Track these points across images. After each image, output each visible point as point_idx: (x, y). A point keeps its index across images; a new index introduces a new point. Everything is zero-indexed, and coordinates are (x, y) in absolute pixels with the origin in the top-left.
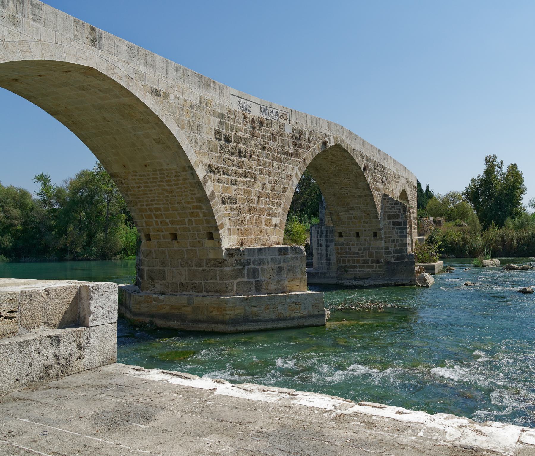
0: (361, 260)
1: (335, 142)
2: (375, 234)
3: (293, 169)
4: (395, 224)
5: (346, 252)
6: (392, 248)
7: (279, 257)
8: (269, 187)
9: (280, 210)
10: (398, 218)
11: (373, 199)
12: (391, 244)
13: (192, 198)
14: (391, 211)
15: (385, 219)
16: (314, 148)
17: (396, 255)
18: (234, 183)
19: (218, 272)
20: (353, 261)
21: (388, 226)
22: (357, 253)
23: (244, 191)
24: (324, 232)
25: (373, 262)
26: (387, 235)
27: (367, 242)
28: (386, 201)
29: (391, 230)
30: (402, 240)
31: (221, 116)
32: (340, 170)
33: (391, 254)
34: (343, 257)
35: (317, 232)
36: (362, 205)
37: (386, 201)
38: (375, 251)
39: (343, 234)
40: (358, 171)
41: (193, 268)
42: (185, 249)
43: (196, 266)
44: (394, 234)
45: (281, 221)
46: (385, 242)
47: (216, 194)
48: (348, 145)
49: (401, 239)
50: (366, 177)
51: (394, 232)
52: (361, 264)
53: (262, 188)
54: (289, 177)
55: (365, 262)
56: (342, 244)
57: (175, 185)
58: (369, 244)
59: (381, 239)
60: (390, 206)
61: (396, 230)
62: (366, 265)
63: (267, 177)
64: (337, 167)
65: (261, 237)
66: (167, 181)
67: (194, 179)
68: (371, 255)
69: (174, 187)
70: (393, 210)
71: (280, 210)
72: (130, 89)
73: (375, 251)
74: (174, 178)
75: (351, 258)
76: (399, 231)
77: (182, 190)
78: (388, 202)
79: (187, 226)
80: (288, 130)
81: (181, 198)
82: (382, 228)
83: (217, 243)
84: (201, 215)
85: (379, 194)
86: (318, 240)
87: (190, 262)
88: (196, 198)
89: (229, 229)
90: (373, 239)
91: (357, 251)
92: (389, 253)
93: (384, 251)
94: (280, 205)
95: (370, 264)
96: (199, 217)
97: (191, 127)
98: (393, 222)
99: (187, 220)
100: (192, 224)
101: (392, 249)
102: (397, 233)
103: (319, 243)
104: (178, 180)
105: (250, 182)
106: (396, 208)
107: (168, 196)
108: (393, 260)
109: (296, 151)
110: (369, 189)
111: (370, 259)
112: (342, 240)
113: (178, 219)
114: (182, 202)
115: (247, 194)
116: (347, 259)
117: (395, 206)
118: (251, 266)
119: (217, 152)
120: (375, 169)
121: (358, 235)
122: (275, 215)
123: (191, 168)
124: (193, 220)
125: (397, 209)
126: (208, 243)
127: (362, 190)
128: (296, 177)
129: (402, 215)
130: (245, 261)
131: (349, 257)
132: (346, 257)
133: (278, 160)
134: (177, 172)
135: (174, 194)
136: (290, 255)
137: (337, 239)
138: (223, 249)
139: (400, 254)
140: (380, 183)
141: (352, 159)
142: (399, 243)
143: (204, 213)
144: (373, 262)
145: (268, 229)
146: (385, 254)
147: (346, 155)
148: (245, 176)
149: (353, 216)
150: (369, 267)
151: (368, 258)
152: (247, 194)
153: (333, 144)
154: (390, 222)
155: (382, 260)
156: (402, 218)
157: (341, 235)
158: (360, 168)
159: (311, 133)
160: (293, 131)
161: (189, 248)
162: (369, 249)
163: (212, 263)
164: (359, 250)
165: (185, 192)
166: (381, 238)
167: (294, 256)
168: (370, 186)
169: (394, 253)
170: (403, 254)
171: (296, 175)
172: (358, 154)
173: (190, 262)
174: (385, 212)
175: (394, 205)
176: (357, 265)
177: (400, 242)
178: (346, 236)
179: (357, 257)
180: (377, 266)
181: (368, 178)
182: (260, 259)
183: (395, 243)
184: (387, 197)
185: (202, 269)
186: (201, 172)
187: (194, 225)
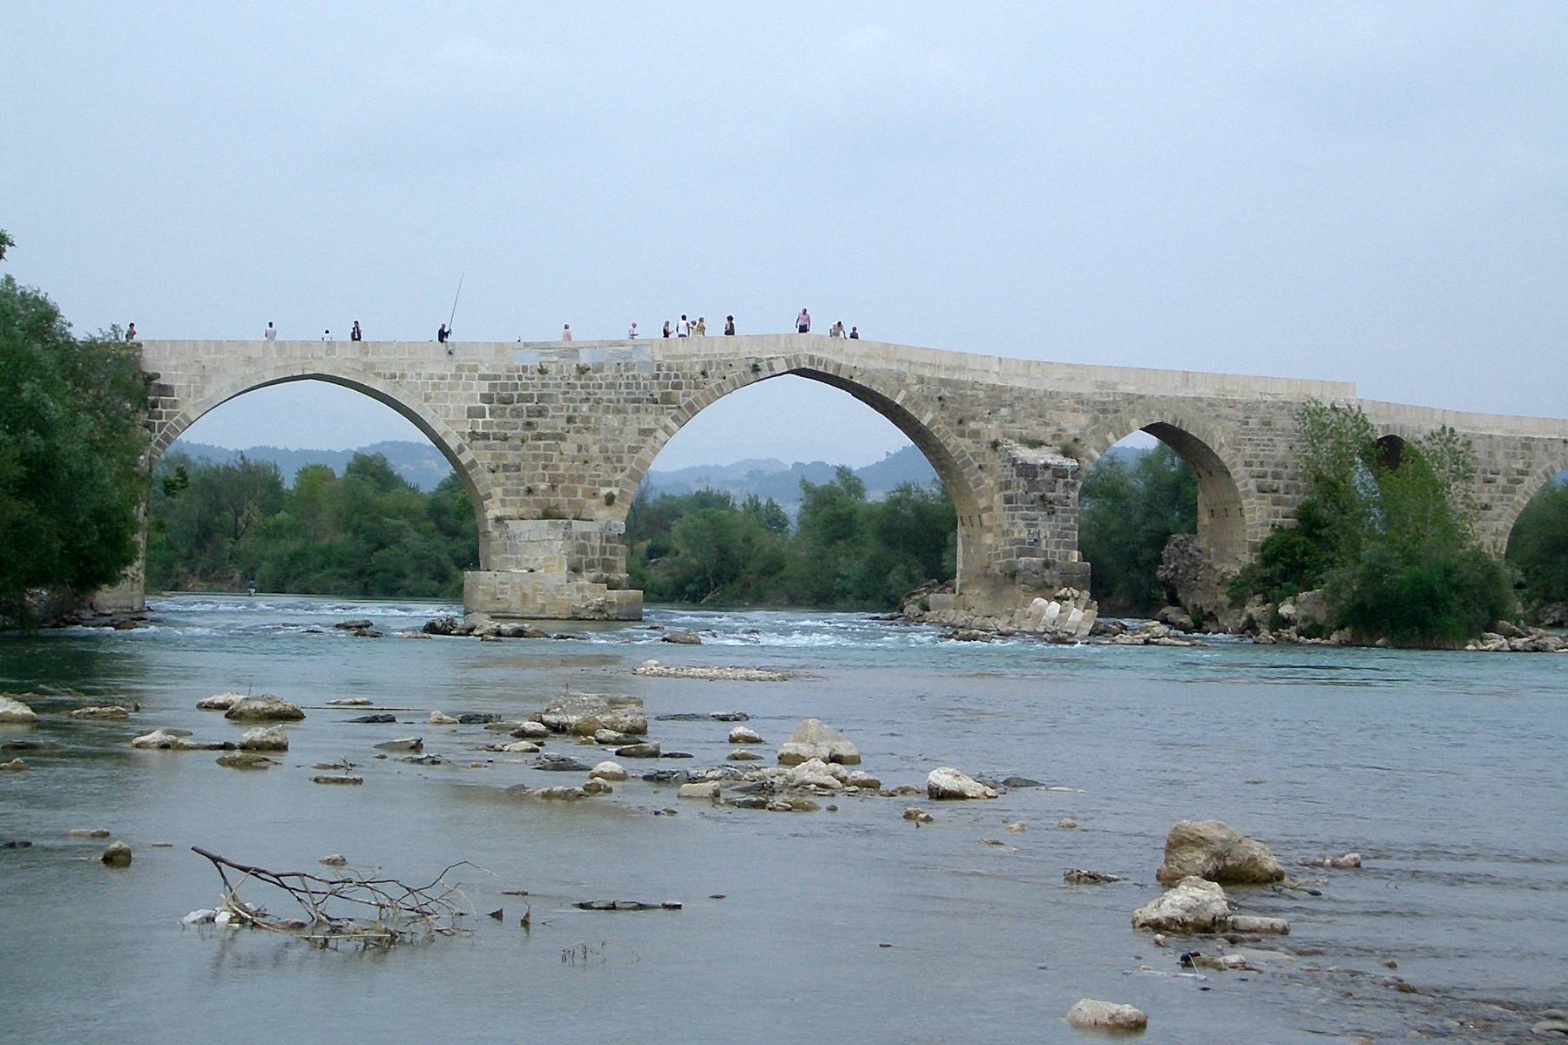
9: (619, 476)
23: (536, 457)
31: (496, 377)
45: (621, 491)
53: (579, 451)
89: (502, 500)
122: (609, 484)
133: (618, 411)
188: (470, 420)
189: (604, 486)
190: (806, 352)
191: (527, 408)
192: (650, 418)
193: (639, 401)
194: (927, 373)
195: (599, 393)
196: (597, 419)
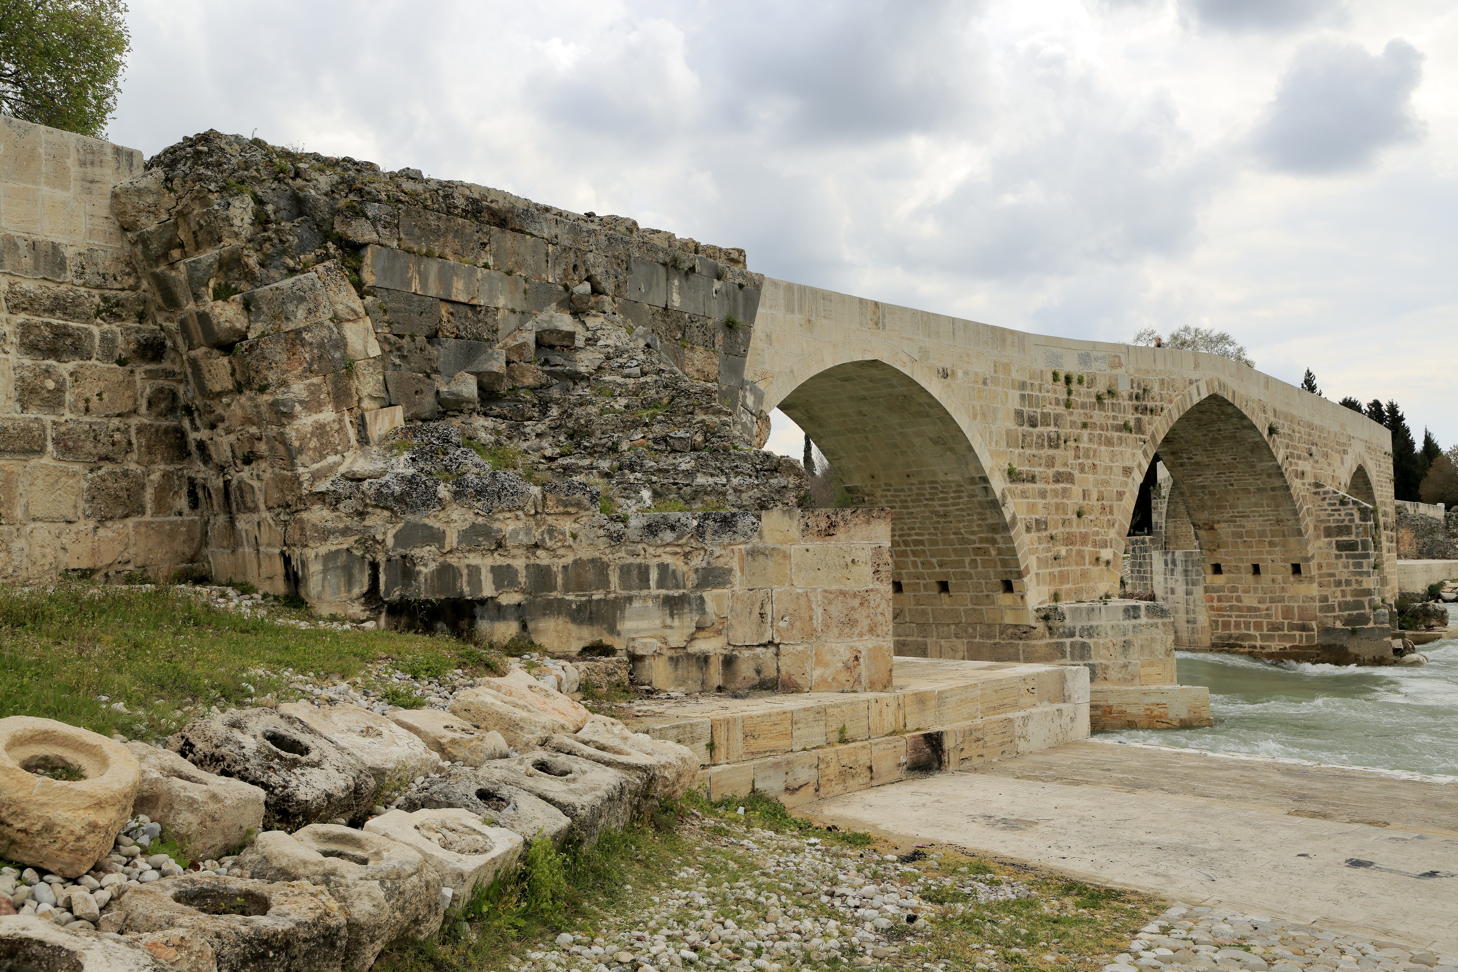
0: (1265, 624)
1: (1208, 390)
2: (1296, 569)
3: (1134, 455)
4: (1340, 546)
5: (1231, 608)
6: (1335, 597)
7: (1126, 623)
8: (1095, 495)
9: (1112, 534)
10: (1349, 533)
11: (1291, 496)
12: (1334, 589)
13: (980, 526)
14: (1331, 518)
15: (1318, 537)
17: (1346, 613)
18: (1043, 494)
19: (1021, 648)
20: (1247, 625)
21: (1326, 551)
22: (1257, 609)
23: (1057, 507)
24: (1178, 563)
25: (1292, 627)
26: (1324, 570)
27: (1277, 586)
28: (1320, 498)
29: (1333, 561)
30: (1358, 582)
31: (1023, 386)
32: (1217, 439)
33: (1334, 610)
34: (1224, 616)
35: (1163, 562)
36: (1266, 509)
37: (1320, 498)
38: (1296, 605)
40: (1257, 440)
41: (977, 640)
42: (962, 608)
43: (981, 636)
44: (1341, 569)
45: (1115, 554)
46: (1321, 585)
47: (1018, 517)
48: (1234, 393)
49: (1357, 580)
50: (1274, 450)
51: (1340, 565)
52: (1265, 632)
55: (1275, 627)
56: (1221, 589)
57: (954, 505)
58: (1283, 589)
59: (1311, 579)
60: (1330, 508)
61: (1344, 560)
62: (1276, 633)
63: (1091, 477)
64: (1211, 435)
65: (1083, 585)
66: (942, 499)
67: (987, 495)
68: (1287, 613)
69: (952, 508)
70: (1337, 517)
71: (1112, 534)
72: (915, 378)
73: (1296, 605)
74: (952, 495)
75: (1242, 619)
76: (1351, 561)
77: (964, 513)
78: (1324, 499)
79: (967, 570)
80: (1124, 389)
81: (961, 525)
82: (1313, 557)
83: (1019, 600)
84: (993, 553)
85: (1304, 484)
86: (1166, 579)
87: (970, 630)
88: (986, 525)
89: (1037, 574)
90: (1292, 579)
91: (1256, 605)
92: (1331, 609)
93: (1317, 604)
95: (1286, 632)
96: (990, 555)
97: (984, 415)
98: (1337, 542)
99: (967, 560)
100: (977, 567)
101: (1336, 600)
102: (1346, 566)
103: (1169, 586)
104: (960, 498)
105: (1065, 490)
106: (1343, 513)
107: (938, 522)
108: (1339, 625)
109: (1138, 421)
110: (1282, 475)
111: (1286, 622)
112: (1220, 580)
113: (953, 558)
114: (962, 531)
115: (1061, 511)
116: (1233, 620)
117: (1342, 508)
118: (1077, 638)
119: (1018, 447)
120: (1294, 431)
121: (1256, 569)
122: (1104, 545)
123: (985, 480)
124: (979, 561)
125: (1347, 515)
126: (1004, 599)
127: (1264, 477)
129: (1357, 528)
130: (1067, 631)
131: (1237, 616)
132: (1230, 616)
133: (1109, 442)
134: (959, 486)
135: (948, 519)
136: (1143, 620)
137: (1211, 579)
138: (1030, 608)
139: (1355, 613)
140: (1305, 459)
141: (1243, 417)
142: (1352, 588)
143: (999, 549)
144: (1292, 627)
145: (1095, 570)
146: (1320, 610)
147: (1230, 410)
148: (1057, 481)
149: (1244, 530)
150: (1283, 638)
151: (1281, 620)
152: (1061, 511)
153: (1204, 395)
154: (1330, 543)
155: (1314, 624)
156: (1357, 535)
157: (1217, 569)
158: (1261, 435)
159: (1162, 382)
161: (970, 606)
162: (1282, 600)
163: (1010, 631)
164: (1259, 602)
165: (969, 515)
166: (1311, 577)
167: (1151, 621)
168: (1283, 470)
169: (1341, 610)
170: (1362, 611)
171: (1140, 465)
172: (1255, 406)
173: (970, 630)
174: (1318, 521)
175: (1337, 507)
176: (1257, 634)
177: (1355, 586)
178: (1230, 571)
179: (1257, 616)
180: (1301, 636)
182: (1091, 627)
183: (1344, 588)
184: (1321, 490)
185: (992, 641)
186: (998, 484)
187: (980, 569)
192: (1128, 451)
196: (1095, 451)
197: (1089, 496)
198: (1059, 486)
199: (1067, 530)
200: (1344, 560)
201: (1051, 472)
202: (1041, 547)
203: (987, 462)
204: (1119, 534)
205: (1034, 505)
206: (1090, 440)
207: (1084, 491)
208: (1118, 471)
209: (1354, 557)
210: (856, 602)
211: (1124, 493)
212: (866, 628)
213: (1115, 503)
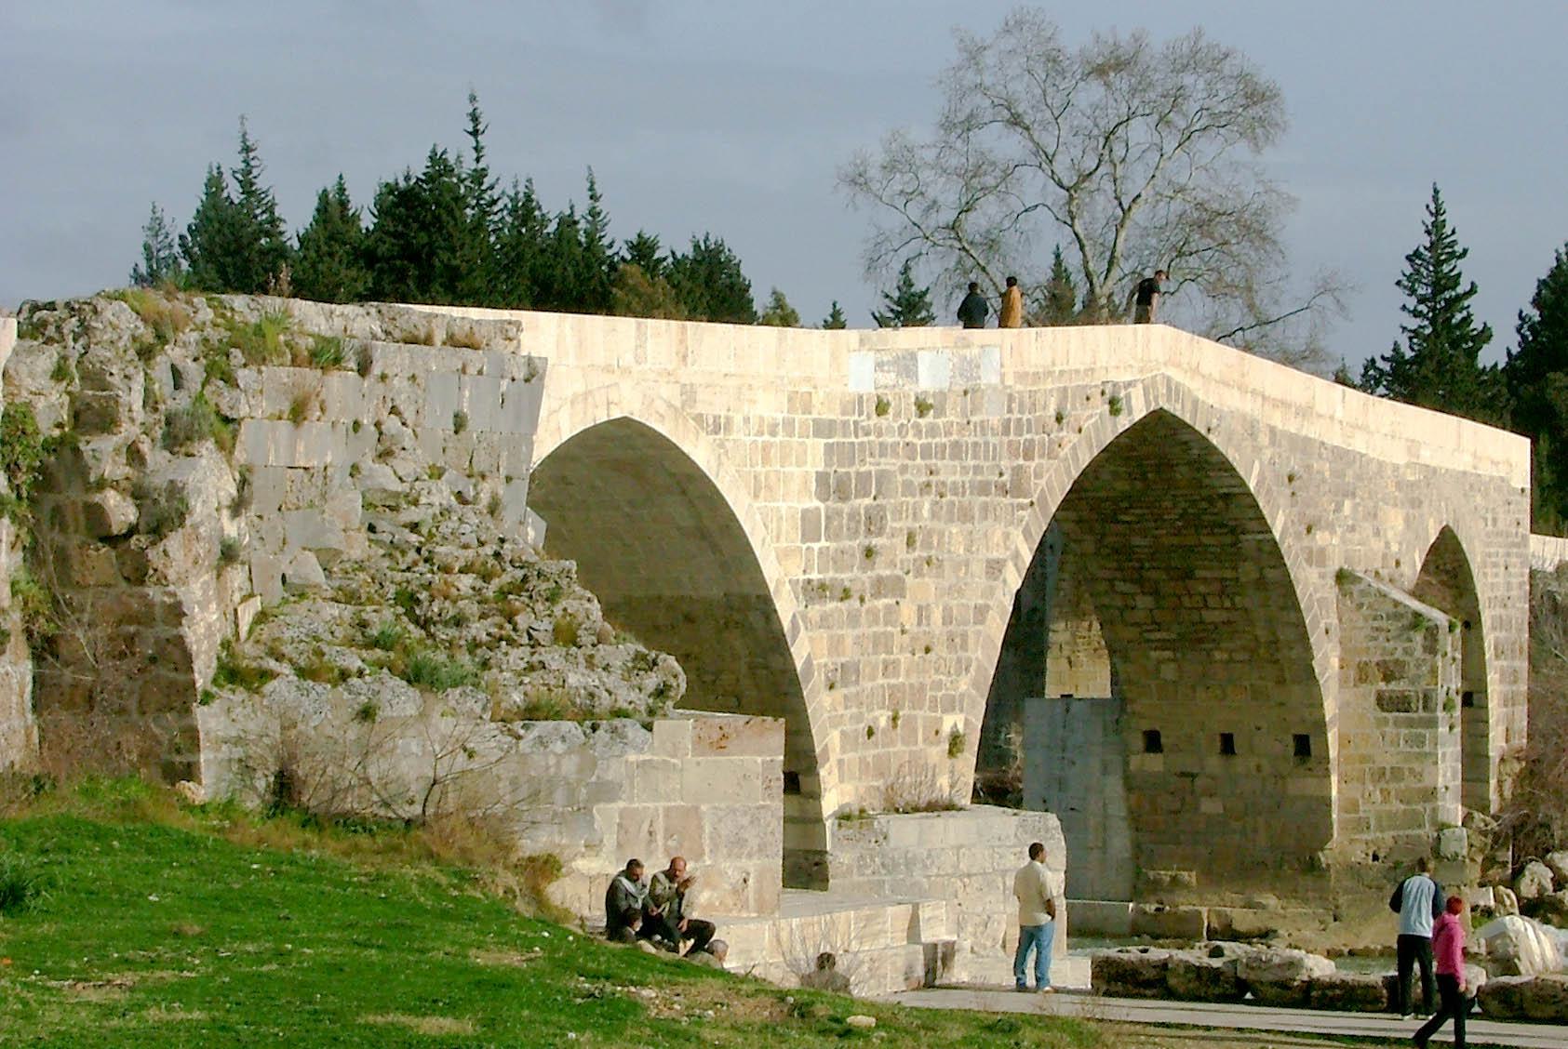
1: (1147, 402)
3: (1007, 536)
4: (1383, 702)
8: (937, 615)
16: (1074, 448)
30: (1418, 776)
39: (1163, 740)
45: (967, 723)
48: (1196, 402)
54: (995, 568)
61: (1389, 729)
71: (964, 685)
76: (1404, 731)
89: (840, 762)
94: (967, 670)
112: (1155, 763)
115: (881, 648)
121: (1227, 745)
122: (951, 705)
128: (1016, 565)
133: (965, 516)
152: (881, 648)
160: (1009, 406)
171: (1016, 556)
175: (1384, 624)
181: (1274, 519)
186: (786, 607)
188: (804, 546)
189: (945, 711)
190: (1163, 370)
191: (867, 509)
193: (983, 489)
194: (1277, 420)
195: (950, 472)
196: (941, 535)
197: (928, 617)
198: (881, 603)
199: (893, 681)
200: (1389, 729)
201: (867, 577)
202: (848, 712)
203: (772, 571)
204: (975, 684)
205: (840, 639)
206: (934, 515)
207: (920, 609)
208: (978, 568)
209: (1410, 724)
210: (745, 821)
211: (987, 607)
212: (756, 848)
213: (971, 629)
